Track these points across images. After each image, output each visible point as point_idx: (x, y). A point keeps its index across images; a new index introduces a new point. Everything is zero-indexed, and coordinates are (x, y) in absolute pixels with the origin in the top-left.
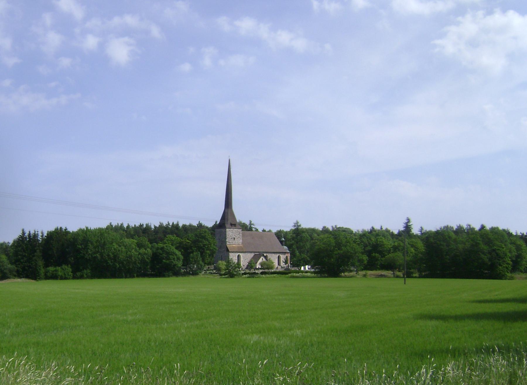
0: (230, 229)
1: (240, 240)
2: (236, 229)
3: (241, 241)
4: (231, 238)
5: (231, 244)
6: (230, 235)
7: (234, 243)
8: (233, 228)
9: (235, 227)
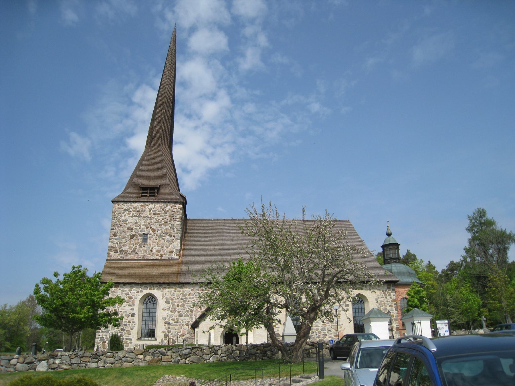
0: (126, 206)
2: (157, 205)
3: (177, 245)
4: (132, 237)
5: (129, 257)
6: (128, 226)
7: (141, 255)
8: (144, 202)
9: (150, 199)
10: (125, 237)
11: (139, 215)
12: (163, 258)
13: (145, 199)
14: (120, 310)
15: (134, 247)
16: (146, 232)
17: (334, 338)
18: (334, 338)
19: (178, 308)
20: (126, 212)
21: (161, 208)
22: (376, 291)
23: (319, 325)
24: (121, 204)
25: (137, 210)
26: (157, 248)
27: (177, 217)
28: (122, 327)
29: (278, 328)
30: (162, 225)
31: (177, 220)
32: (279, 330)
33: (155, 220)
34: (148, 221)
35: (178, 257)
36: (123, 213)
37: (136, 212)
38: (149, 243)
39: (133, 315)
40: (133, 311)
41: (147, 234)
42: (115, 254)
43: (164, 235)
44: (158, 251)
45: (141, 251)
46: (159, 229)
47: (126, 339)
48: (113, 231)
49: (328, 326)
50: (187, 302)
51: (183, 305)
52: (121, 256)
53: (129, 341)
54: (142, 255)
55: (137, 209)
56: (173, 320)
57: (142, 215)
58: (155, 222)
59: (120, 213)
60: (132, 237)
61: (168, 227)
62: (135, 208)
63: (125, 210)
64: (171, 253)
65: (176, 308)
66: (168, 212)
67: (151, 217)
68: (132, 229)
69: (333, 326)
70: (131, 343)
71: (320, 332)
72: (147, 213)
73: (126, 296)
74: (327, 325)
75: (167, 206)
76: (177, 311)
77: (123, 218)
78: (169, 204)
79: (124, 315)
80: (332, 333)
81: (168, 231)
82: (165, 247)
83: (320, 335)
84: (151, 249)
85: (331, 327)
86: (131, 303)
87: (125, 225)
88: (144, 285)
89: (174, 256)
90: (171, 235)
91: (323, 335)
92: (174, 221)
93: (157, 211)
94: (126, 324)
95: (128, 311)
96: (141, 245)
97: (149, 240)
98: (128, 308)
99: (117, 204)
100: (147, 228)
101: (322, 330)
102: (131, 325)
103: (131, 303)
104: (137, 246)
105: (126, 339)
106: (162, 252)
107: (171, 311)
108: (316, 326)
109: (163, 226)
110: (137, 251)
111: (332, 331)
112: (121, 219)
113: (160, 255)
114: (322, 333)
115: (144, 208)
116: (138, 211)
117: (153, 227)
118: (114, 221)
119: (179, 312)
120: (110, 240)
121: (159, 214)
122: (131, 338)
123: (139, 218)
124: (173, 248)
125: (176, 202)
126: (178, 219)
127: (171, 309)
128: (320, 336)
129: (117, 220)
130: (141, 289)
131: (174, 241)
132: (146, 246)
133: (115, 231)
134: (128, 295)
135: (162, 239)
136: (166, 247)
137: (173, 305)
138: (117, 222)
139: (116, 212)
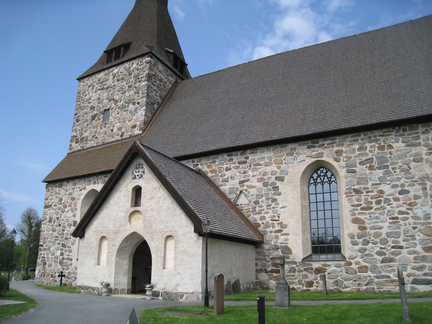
1: (133, 113)
2: (121, 68)
4: (93, 118)
5: (90, 144)
10: (87, 121)
11: (102, 87)
12: (124, 137)
13: (109, 65)
14: (62, 218)
15: (95, 130)
16: (108, 107)
17: (425, 254)
18: (425, 254)
20: (90, 88)
21: (126, 70)
23: (381, 224)
24: (86, 80)
25: (101, 82)
26: (118, 125)
27: (142, 76)
28: (63, 242)
29: (287, 234)
30: (125, 92)
31: (143, 79)
32: (288, 240)
33: (118, 88)
34: (111, 92)
35: (141, 132)
36: (88, 90)
37: (99, 85)
38: (110, 121)
40: (75, 218)
41: (109, 110)
42: (76, 144)
43: (126, 105)
44: (120, 129)
45: (101, 134)
46: (122, 98)
47: (67, 259)
48: (76, 115)
49: (405, 225)
52: (81, 145)
53: (70, 262)
54: (103, 138)
55: (100, 80)
58: (119, 91)
59: (85, 92)
60: (93, 118)
61: (132, 92)
62: (99, 80)
63: (89, 86)
64: (134, 128)
66: (133, 73)
67: (114, 86)
68: (94, 107)
69: (419, 226)
71: (384, 242)
72: (110, 83)
73: (69, 197)
74: (402, 223)
75: (133, 64)
77: (87, 97)
78: (134, 61)
79: (66, 225)
80: (417, 242)
81: (132, 98)
82: (127, 121)
83: (384, 248)
84: (112, 128)
85: (414, 228)
86: (73, 206)
87: (88, 104)
88: (88, 179)
89: (137, 131)
90: (135, 102)
91: (393, 247)
92: (139, 82)
93: (121, 75)
94: (67, 237)
96: (102, 125)
97: (111, 116)
98: (70, 214)
99: (82, 82)
100: (109, 101)
101: (388, 235)
103: (73, 206)
104: (97, 129)
105: (67, 259)
106: (123, 130)
108: (373, 228)
110: (97, 136)
111: (417, 237)
112: (85, 100)
113: (120, 135)
114: (390, 243)
115: (107, 77)
116: (101, 83)
117: (116, 97)
118: (79, 103)
120: (73, 128)
121: (122, 79)
122: (72, 257)
123: (102, 91)
124: (137, 120)
125: (142, 56)
126: (144, 78)
128: (384, 251)
129: (81, 102)
130: (84, 184)
131: (138, 109)
132: (107, 126)
133: (78, 115)
134: (71, 196)
135: (124, 111)
136: (128, 121)
138: (82, 104)
139: (81, 92)
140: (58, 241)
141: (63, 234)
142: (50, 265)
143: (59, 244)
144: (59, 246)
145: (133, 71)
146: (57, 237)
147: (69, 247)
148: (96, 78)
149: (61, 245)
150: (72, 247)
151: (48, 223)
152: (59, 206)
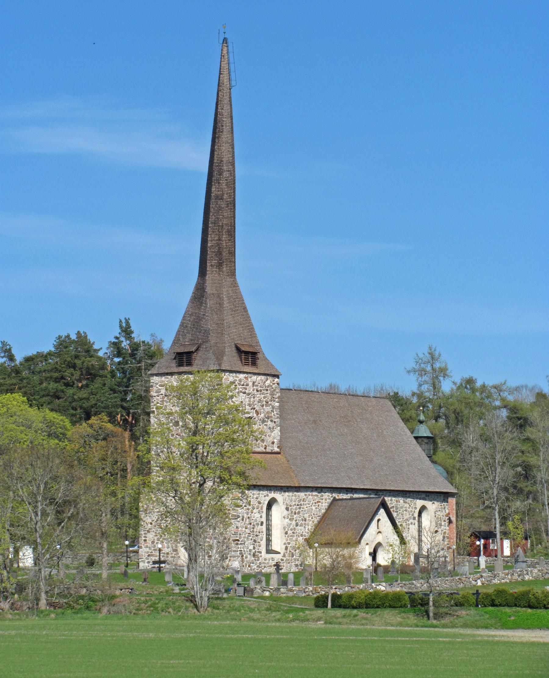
1: (272, 429)
2: (259, 378)
8: (247, 373)
14: (252, 518)
19: (295, 516)
22: (435, 502)
39: (262, 524)
47: (258, 552)
50: (302, 509)
51: (299, 513)
53: (260, 555)
56: (291, 530)
57: (247, 391)
62: (240, 381)
65: (293, 516)
70: (261, 556)
75: (267, 379)
76: (295, 519)
78: (268, 377)
79: (255, 524)
95: (258, 519)
98: (257, 515)
102: (260, 536)
107: (290, 520)
109: (264, 407)
116: (242, 385)
119: (296, 520)
124: (274, 438)
127: (290, 517)
135: (265, 425)
137: (292, 512)
140: (251, 537)
141: (253, 531)
142: (246, 557)
143: (251, 539)
144: (251, 541)
145: (268, 386)
146: (249, 534)
147: (259, 542)
148: (236, 377)
149: (253, 541)
150: (261, 542)
151: (241, 521)
152: (248, 507)
